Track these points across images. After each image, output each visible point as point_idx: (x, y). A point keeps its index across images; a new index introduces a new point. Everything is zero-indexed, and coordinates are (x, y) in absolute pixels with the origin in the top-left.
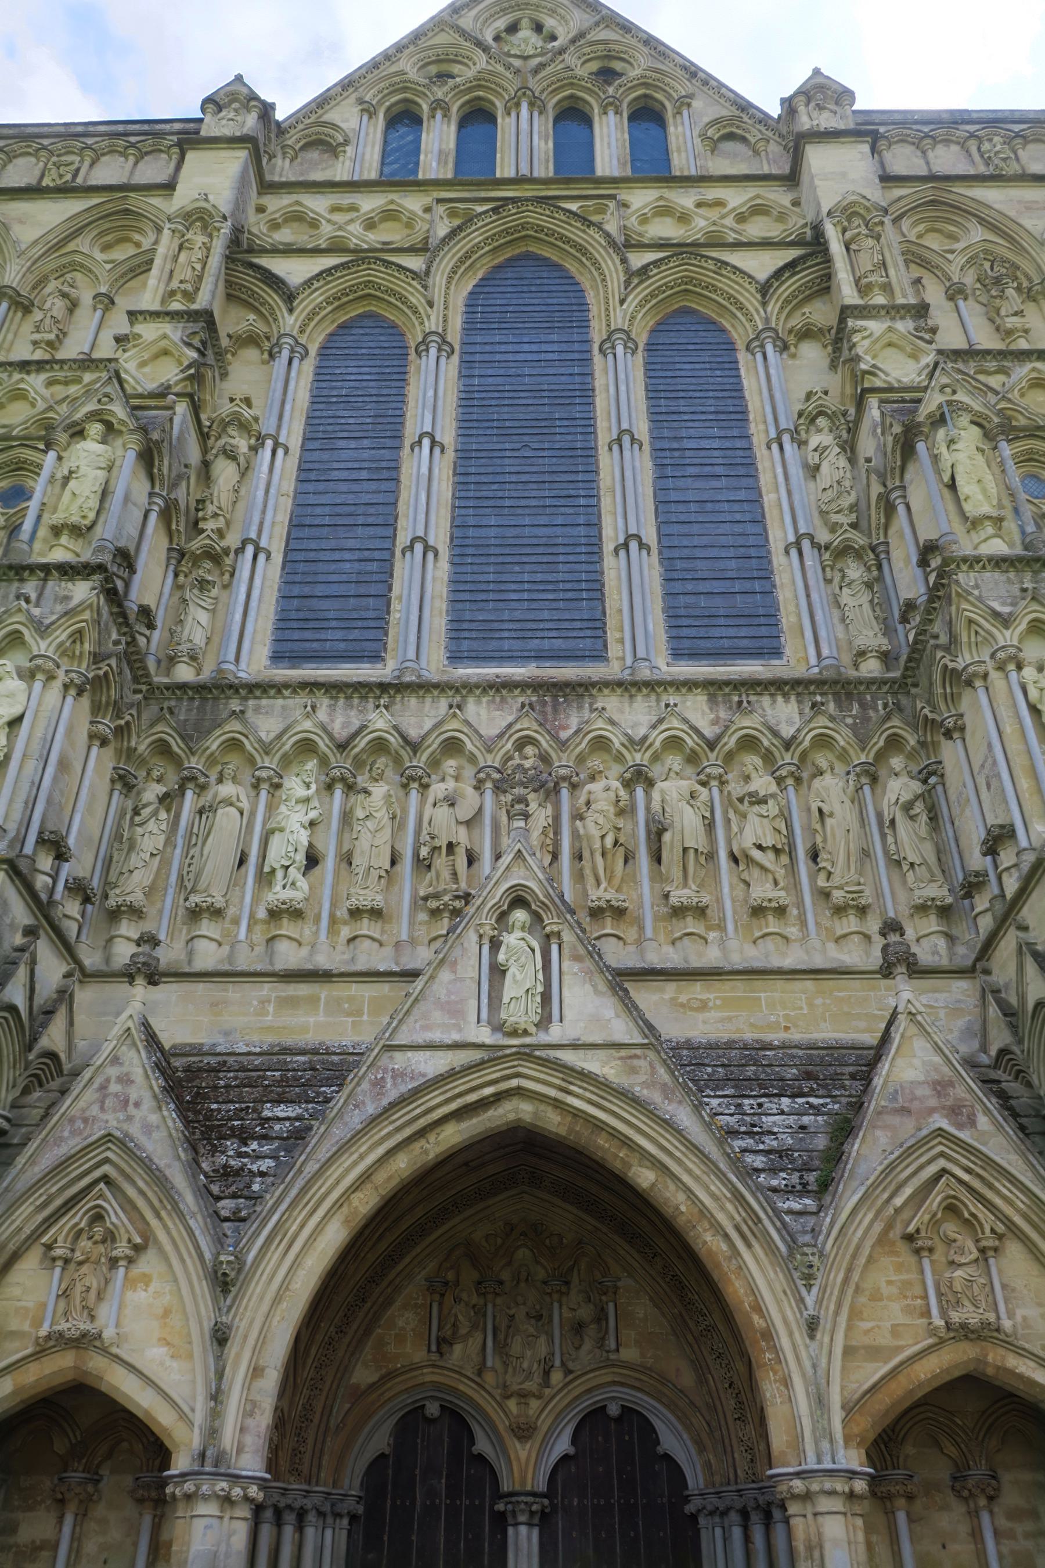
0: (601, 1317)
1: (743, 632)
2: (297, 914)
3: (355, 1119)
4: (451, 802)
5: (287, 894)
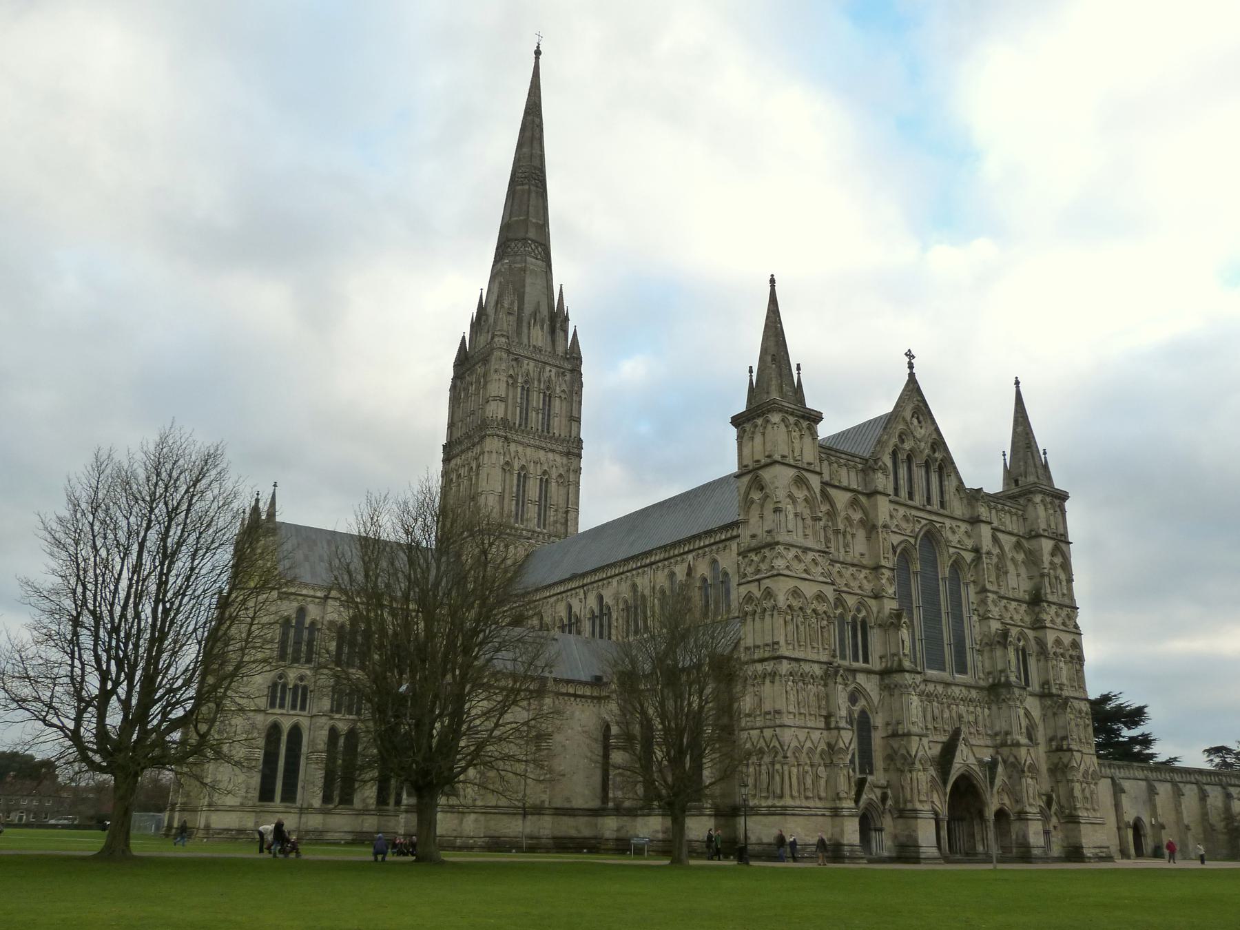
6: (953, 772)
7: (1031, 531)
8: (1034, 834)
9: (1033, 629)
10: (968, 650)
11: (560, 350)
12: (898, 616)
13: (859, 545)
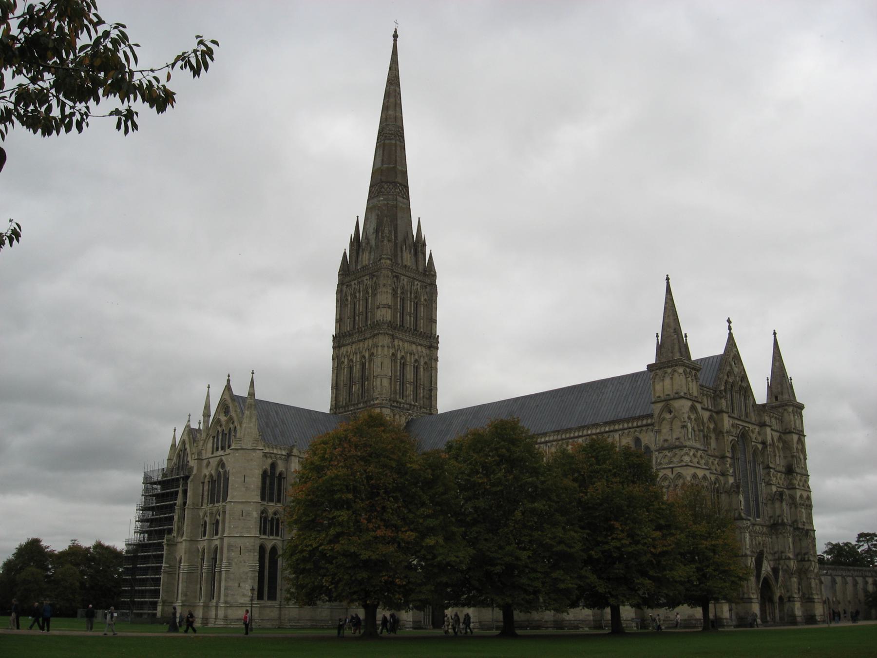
6: (762, 576)
7: (786, 429)
9: (788, 489)
11: (421, 268)
12: (738, 487)
13: (713, 444)
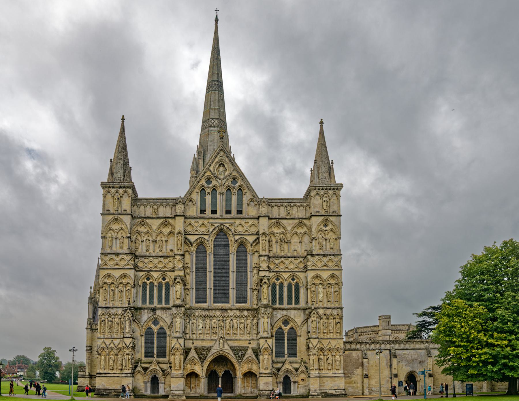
0: (226, 364)
1: (243, 299)
2: (201, 334)
3: (210, 355)
4: (215, 323)
5: (201, 332)
8: (264, 384)
10: (248, 290)
